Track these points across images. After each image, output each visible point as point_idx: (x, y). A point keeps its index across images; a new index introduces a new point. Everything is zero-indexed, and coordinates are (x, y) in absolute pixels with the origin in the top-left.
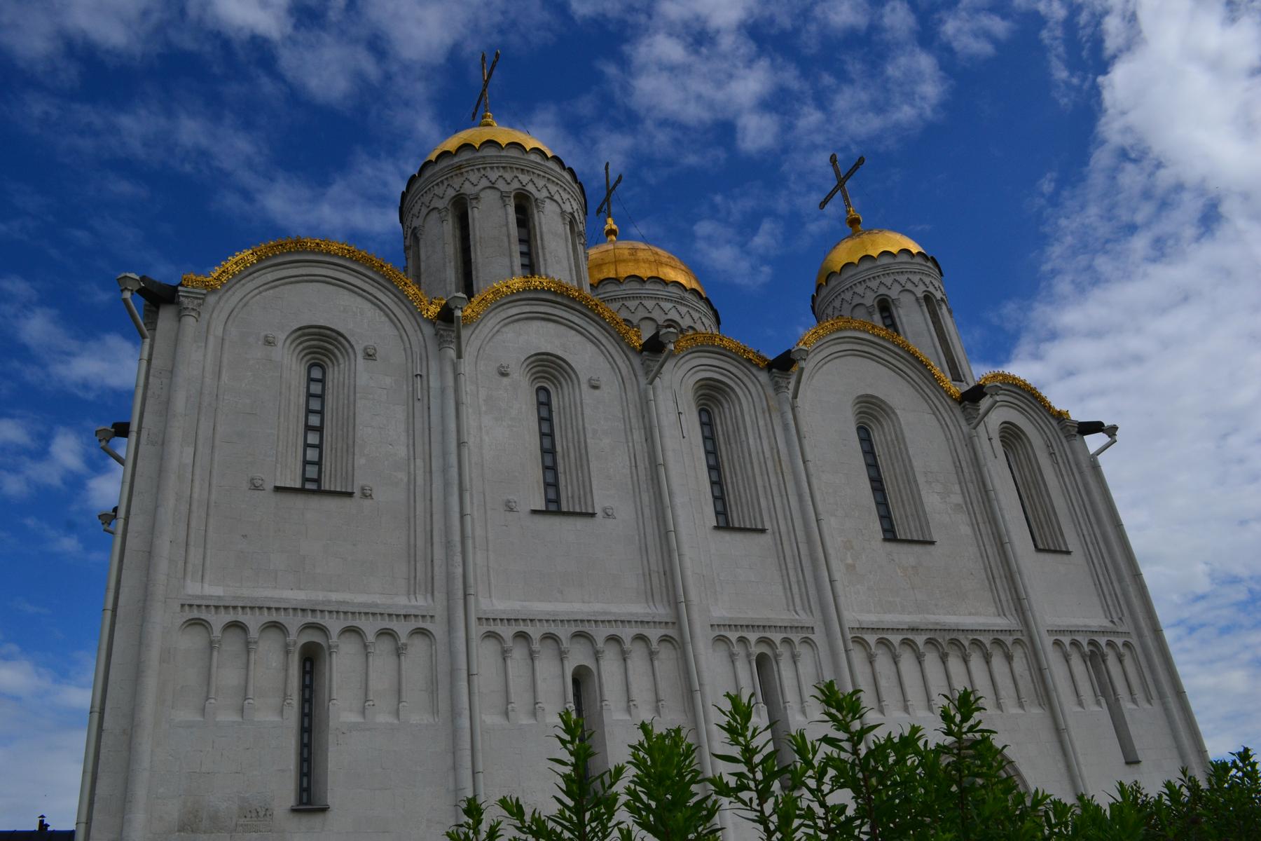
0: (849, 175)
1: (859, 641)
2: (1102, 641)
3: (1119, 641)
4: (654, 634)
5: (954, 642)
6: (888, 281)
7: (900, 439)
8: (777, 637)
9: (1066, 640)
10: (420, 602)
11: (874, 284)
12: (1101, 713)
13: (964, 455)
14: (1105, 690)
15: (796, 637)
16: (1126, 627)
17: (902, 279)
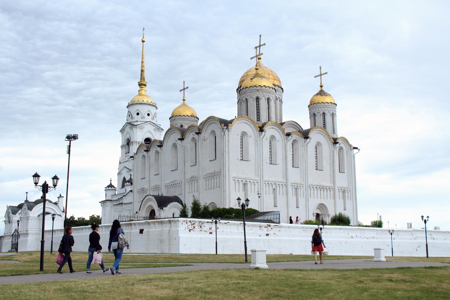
0: (324, 74)
1: (310, 187)
2: (346, 189)
3: (348, 190)
4: (283, 184)
5: (323, 188)
6: (326, 109)
7: (322, 150)
8: (299, 185)
9: (340, 189)
10: (257, 178)
11: (323, 109)
12: (342, 201)
13: (332, 154)
14: (344, 198)
15: (301, 186)
16: (351, 187)
17: (329, 109)
